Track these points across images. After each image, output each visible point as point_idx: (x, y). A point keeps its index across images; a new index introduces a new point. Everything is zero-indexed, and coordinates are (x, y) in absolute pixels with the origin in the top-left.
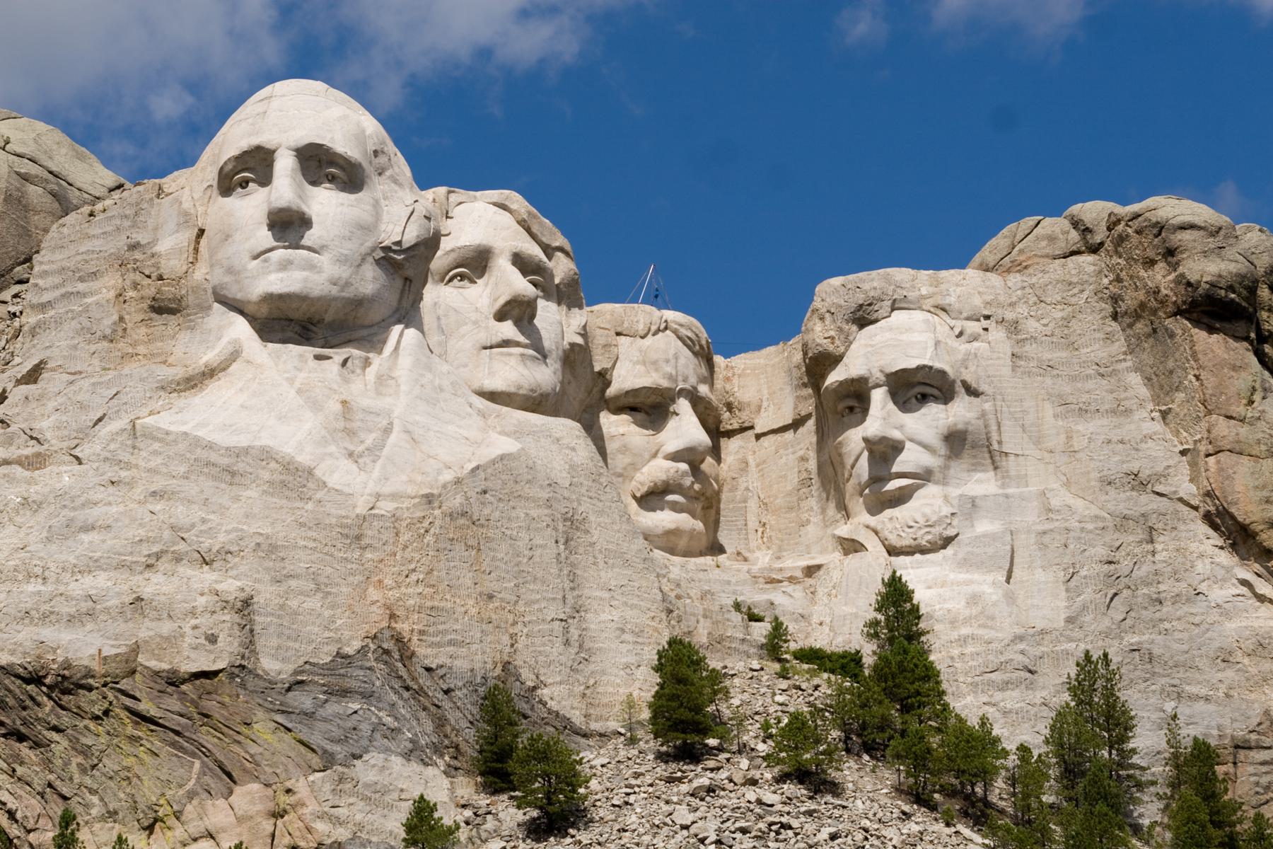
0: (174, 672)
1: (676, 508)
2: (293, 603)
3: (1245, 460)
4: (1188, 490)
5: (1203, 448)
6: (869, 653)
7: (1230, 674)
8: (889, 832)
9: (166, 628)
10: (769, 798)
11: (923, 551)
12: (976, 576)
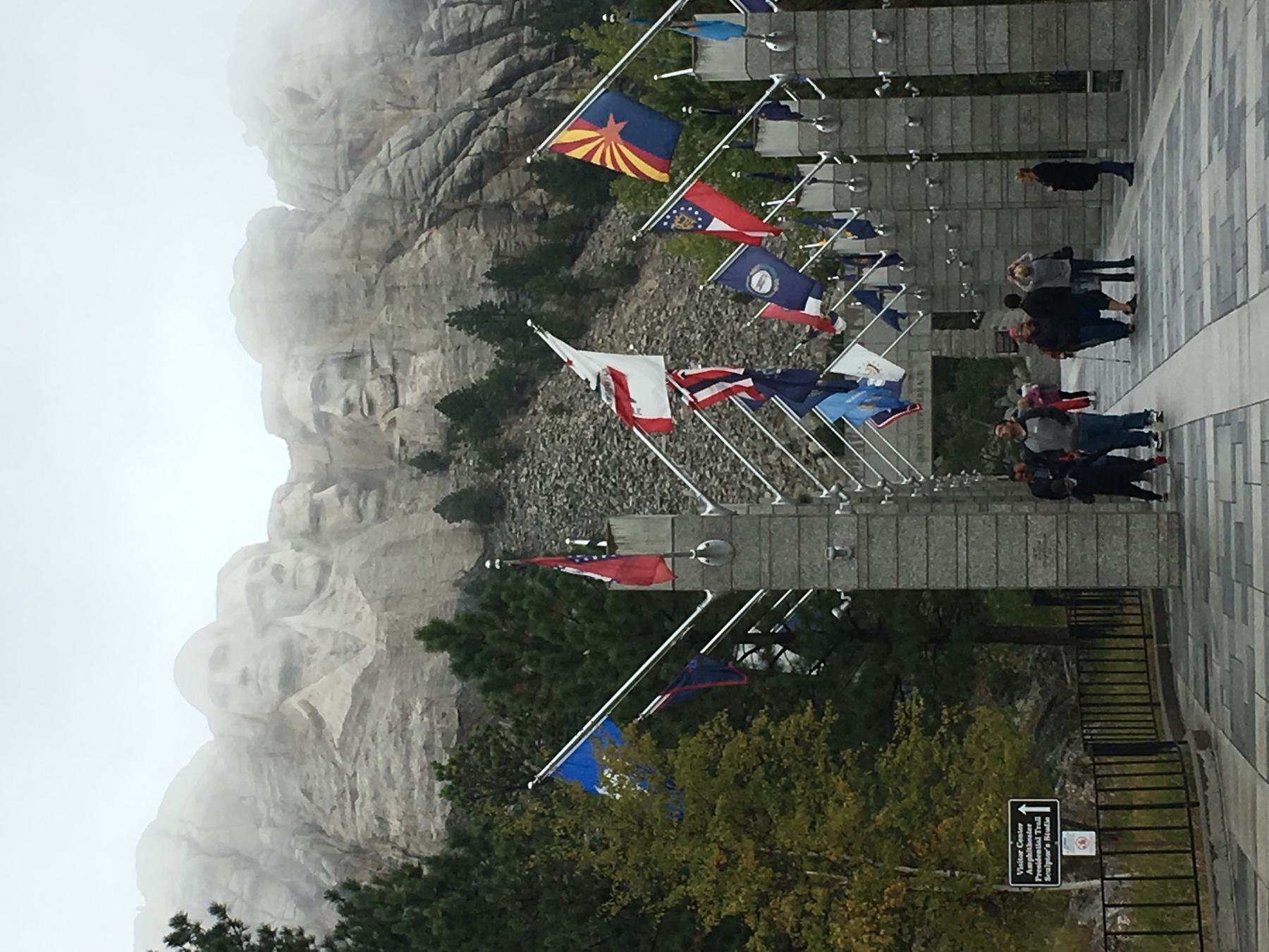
0: (458, 732)
1: (365, 502)
2: (427, 679)
3: (364, 242)
4: (374, 269)
5: (356, 261)
6: (443, 418)
7: (463, 256)
8: (544, 421)
9: (438, 735)
10: (525, 471)
11: (396, 392)
12: (412, 369)
